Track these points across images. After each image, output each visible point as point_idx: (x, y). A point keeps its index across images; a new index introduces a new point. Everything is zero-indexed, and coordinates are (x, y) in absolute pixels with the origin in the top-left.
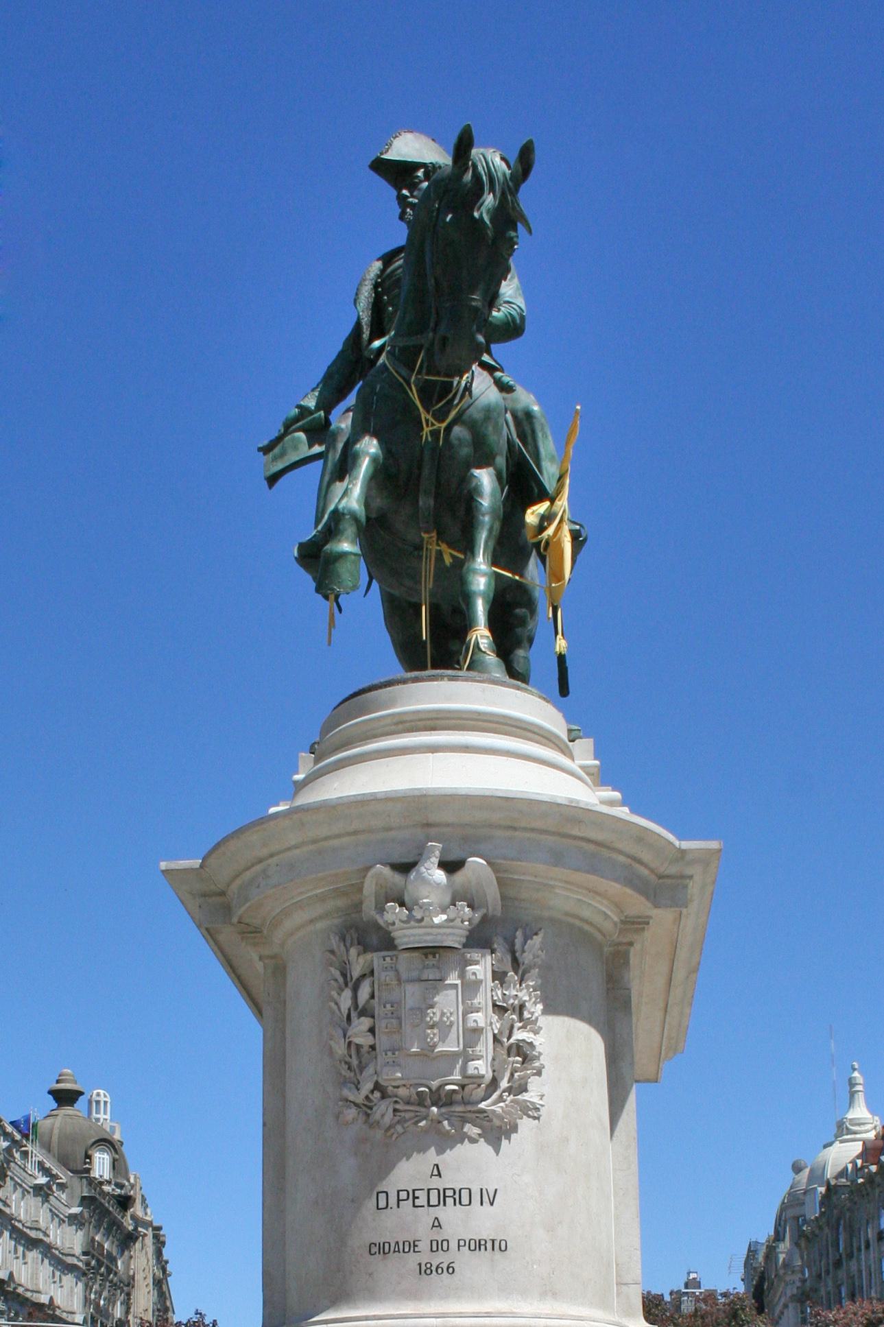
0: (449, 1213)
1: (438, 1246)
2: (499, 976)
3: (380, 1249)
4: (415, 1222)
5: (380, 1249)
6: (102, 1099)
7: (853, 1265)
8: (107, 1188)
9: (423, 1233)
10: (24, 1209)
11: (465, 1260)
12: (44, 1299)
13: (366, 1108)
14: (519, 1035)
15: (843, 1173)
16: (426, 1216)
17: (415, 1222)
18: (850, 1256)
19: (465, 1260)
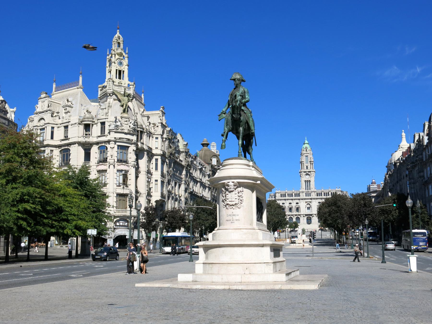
0: (234, 217)
1: (233, 220)
2: (238, 193)
3: (227, 220)
4: (230, 218)
5: (227, 220)
6: (214, 144)
7: (401, 182)
8: (215, 167)
9: (231, 219)
10: (197, 174)
11: (235, 221)
12: (201, 195)
13: (226, 206)
14: (241, 199)
15: (399, 159)
16: (232, 217)
17: (230, 218)
18: (400, 180)
19: (235, 221)
